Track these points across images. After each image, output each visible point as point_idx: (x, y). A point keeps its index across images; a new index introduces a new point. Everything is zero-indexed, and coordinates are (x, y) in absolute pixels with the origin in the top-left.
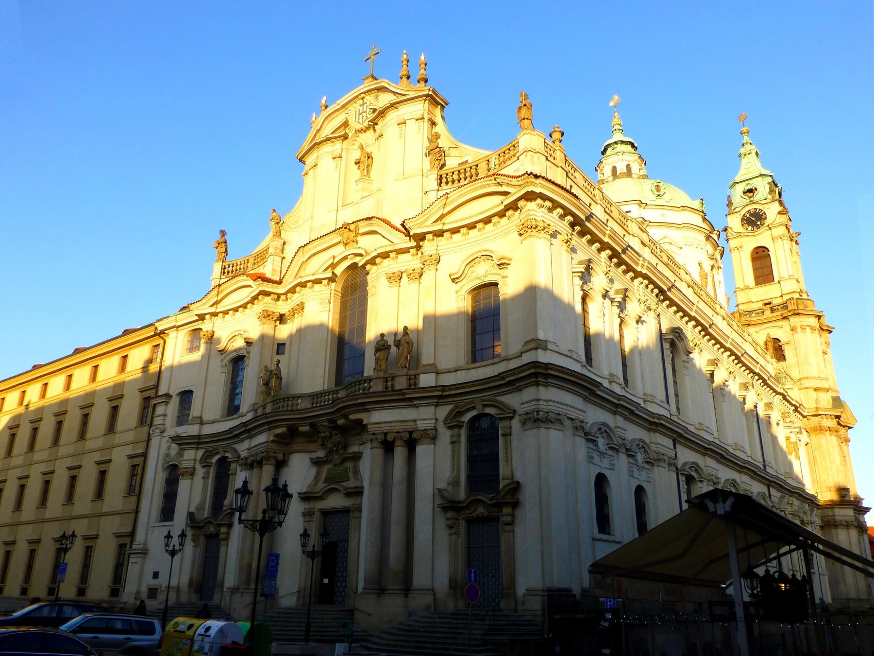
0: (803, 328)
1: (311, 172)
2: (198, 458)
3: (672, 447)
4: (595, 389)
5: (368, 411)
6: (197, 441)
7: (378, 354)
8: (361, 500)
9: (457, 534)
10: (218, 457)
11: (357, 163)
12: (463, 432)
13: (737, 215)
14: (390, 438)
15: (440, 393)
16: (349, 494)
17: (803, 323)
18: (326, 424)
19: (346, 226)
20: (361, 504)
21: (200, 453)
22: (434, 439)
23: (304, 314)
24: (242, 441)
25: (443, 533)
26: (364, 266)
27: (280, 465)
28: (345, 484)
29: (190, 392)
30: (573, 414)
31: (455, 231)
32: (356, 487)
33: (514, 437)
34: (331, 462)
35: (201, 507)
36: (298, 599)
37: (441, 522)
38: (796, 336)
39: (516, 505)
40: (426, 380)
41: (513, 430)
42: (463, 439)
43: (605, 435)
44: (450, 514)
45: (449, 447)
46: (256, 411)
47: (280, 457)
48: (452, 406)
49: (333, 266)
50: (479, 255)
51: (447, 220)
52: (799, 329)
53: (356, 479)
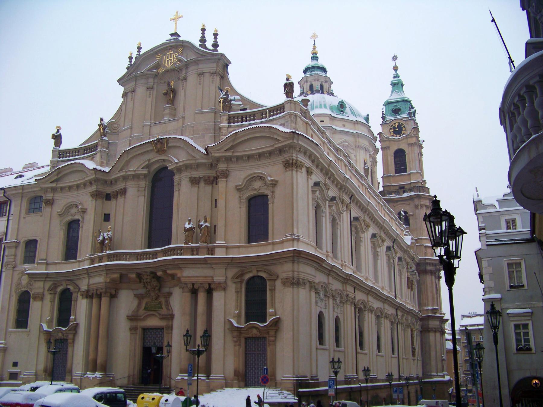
0: (422, 206)
1: (130, 94)
2: (47, 288)
3: (353, 292)
4: (321, 263)
5: (180, 268)
8: (172, 322)
9: (240, 345)
11: (165, 94)
13: (388, 125)
14: (196, 287)
16: (163, 318)
17: (422, 203)
20: (172, 325)
21: (48, 285)
22: (224, 289)
23: (126, 196)
25: (230, 344)
27: (113, 296)
29: (36, 241)
30: (310, 278)
31: (239, 158)
32: (170, 315)
33: (277, 291)
36: (129, 380)
37: (229, 338)
38: (417, 211)
39: (277, 331)
41: (277, 287)
42: (244, 290)
43: (323, 289)
45: (235, 294)
47: (113, 292)
49: (148, 166)
50: (256, 175)
52: (419, 207)
53: (168, 309)
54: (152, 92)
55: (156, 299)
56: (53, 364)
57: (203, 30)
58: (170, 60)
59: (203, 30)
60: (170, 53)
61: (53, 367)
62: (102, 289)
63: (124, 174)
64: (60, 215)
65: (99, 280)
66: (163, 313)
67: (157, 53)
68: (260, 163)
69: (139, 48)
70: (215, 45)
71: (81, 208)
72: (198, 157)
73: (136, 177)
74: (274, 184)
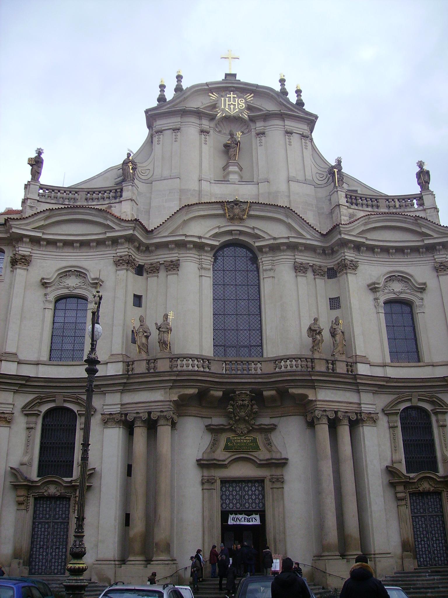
5: (314, 388)
6: (20, 384)
7: (318, 336)
10: (52, 405)
11: (227, 146)
12: (398, 418)
15: (385, 383)
18: (248, 392)
19: (236, 203)
23: (179, 273)
24: (104, 393)
25: (392, 505)
26: (260, 248)
27: (173, 425)
28: (255, 454)
31: (371, 249)
34: (234, 431)
35: (29, 464)
37: (390, 494)
40: (362, 369)
44: (400, 488)
46: (129, 364)
48: (396, 396)
49: (216, 236)
50: (397, 274)
51: (369, 236)
54: (207, 137)
55: (249, 432)
56: (32, 542)
57: (282, 81)
58: (233, 105)
59: (282, 81)
60: (232, 96)
61: (32, 549)
62: (162, 412)
63: (183, 238)
64: (46, 283)
65: (155, 398)
66: (261, 457)
67: (211, 90)
68: (396, 260)
69: (179, 78)
70: (300, 103)
71: (93, 279)
72: (309, 237)
73: (200, 247)
74: (422, 289)
